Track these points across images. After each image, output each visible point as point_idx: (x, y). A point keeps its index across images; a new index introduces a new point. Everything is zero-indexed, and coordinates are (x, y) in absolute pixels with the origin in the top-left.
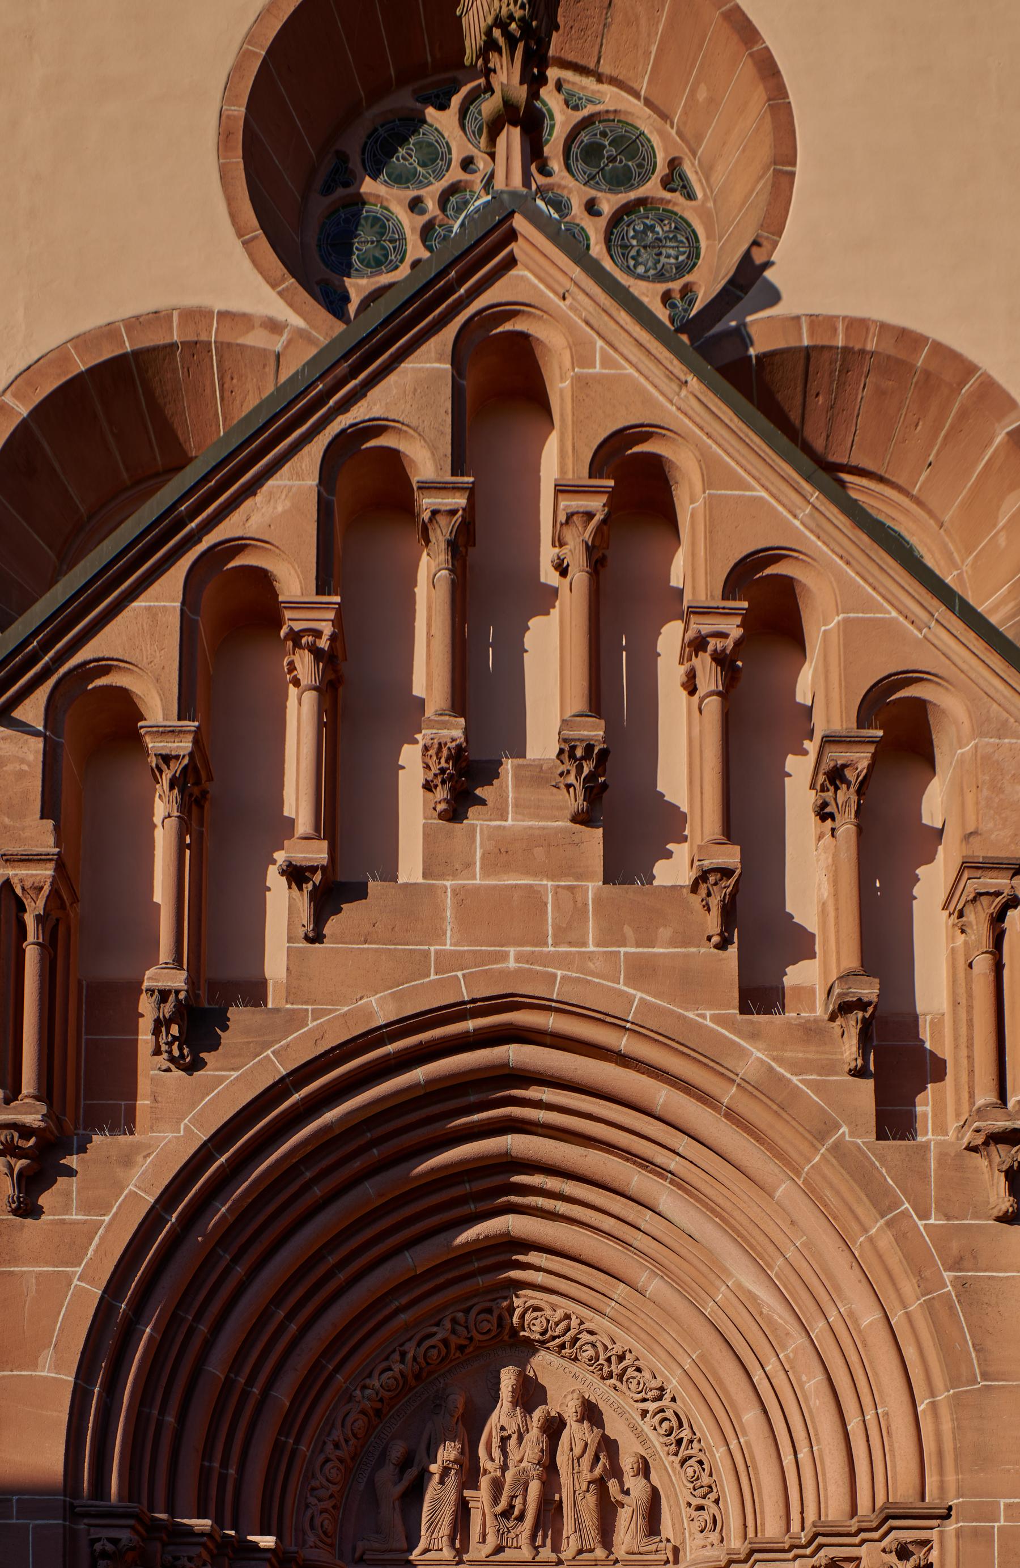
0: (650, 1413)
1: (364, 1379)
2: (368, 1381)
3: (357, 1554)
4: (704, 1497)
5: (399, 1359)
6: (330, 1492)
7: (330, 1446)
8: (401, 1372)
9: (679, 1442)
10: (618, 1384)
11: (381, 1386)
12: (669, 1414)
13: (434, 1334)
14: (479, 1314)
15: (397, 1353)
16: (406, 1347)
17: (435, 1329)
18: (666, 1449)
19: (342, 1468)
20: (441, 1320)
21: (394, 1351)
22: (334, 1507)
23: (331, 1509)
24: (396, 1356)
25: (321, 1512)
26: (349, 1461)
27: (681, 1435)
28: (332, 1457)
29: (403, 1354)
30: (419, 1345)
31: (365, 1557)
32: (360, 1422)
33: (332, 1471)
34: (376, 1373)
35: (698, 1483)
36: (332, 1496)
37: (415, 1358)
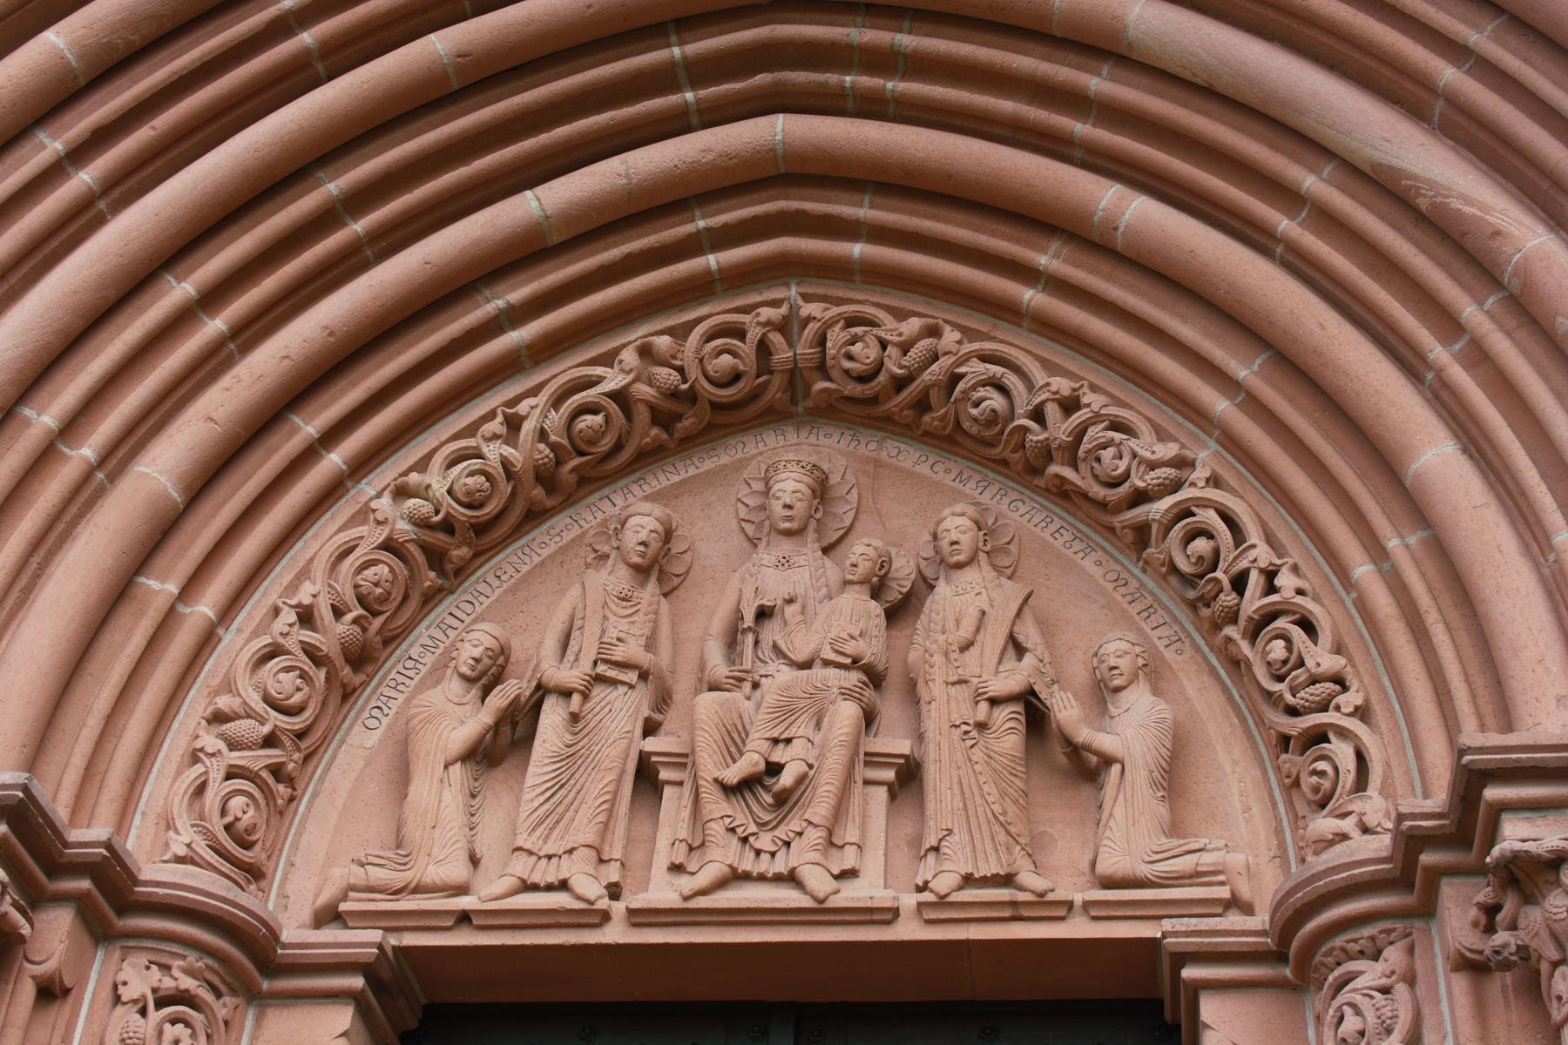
0: (1155, 527)
1: (406, 473)
2: (414, 478)
3: (323, 899)
4: (1325, 709)
5: (503, 430)
6: (266, 729)
8: (506, 464)
9: (1239, 583)
10: (1068, 473)
11: (449, 492)
12: (1211, 518)
13: (596, 381)
14: (710, 338)
15: (500, 418)
16: (523, 407)
17: (599, 370)
18: (1205, 612)
20: (616, 352)
21: (491, 416)
22: (277, 771)
23: (265, 774)
24: (496, 426)
25: (229, 777)
26: (339, 661)
27: (1243, 564)
28: (290, 644)
29: (514, 424)
30: (557, 402)
31: (343, 907)
32: (383, 570)
33: (282, 676)
34: (438, 460)
35: (1300, 675)
36: (270, 741)
37: (542, 435)
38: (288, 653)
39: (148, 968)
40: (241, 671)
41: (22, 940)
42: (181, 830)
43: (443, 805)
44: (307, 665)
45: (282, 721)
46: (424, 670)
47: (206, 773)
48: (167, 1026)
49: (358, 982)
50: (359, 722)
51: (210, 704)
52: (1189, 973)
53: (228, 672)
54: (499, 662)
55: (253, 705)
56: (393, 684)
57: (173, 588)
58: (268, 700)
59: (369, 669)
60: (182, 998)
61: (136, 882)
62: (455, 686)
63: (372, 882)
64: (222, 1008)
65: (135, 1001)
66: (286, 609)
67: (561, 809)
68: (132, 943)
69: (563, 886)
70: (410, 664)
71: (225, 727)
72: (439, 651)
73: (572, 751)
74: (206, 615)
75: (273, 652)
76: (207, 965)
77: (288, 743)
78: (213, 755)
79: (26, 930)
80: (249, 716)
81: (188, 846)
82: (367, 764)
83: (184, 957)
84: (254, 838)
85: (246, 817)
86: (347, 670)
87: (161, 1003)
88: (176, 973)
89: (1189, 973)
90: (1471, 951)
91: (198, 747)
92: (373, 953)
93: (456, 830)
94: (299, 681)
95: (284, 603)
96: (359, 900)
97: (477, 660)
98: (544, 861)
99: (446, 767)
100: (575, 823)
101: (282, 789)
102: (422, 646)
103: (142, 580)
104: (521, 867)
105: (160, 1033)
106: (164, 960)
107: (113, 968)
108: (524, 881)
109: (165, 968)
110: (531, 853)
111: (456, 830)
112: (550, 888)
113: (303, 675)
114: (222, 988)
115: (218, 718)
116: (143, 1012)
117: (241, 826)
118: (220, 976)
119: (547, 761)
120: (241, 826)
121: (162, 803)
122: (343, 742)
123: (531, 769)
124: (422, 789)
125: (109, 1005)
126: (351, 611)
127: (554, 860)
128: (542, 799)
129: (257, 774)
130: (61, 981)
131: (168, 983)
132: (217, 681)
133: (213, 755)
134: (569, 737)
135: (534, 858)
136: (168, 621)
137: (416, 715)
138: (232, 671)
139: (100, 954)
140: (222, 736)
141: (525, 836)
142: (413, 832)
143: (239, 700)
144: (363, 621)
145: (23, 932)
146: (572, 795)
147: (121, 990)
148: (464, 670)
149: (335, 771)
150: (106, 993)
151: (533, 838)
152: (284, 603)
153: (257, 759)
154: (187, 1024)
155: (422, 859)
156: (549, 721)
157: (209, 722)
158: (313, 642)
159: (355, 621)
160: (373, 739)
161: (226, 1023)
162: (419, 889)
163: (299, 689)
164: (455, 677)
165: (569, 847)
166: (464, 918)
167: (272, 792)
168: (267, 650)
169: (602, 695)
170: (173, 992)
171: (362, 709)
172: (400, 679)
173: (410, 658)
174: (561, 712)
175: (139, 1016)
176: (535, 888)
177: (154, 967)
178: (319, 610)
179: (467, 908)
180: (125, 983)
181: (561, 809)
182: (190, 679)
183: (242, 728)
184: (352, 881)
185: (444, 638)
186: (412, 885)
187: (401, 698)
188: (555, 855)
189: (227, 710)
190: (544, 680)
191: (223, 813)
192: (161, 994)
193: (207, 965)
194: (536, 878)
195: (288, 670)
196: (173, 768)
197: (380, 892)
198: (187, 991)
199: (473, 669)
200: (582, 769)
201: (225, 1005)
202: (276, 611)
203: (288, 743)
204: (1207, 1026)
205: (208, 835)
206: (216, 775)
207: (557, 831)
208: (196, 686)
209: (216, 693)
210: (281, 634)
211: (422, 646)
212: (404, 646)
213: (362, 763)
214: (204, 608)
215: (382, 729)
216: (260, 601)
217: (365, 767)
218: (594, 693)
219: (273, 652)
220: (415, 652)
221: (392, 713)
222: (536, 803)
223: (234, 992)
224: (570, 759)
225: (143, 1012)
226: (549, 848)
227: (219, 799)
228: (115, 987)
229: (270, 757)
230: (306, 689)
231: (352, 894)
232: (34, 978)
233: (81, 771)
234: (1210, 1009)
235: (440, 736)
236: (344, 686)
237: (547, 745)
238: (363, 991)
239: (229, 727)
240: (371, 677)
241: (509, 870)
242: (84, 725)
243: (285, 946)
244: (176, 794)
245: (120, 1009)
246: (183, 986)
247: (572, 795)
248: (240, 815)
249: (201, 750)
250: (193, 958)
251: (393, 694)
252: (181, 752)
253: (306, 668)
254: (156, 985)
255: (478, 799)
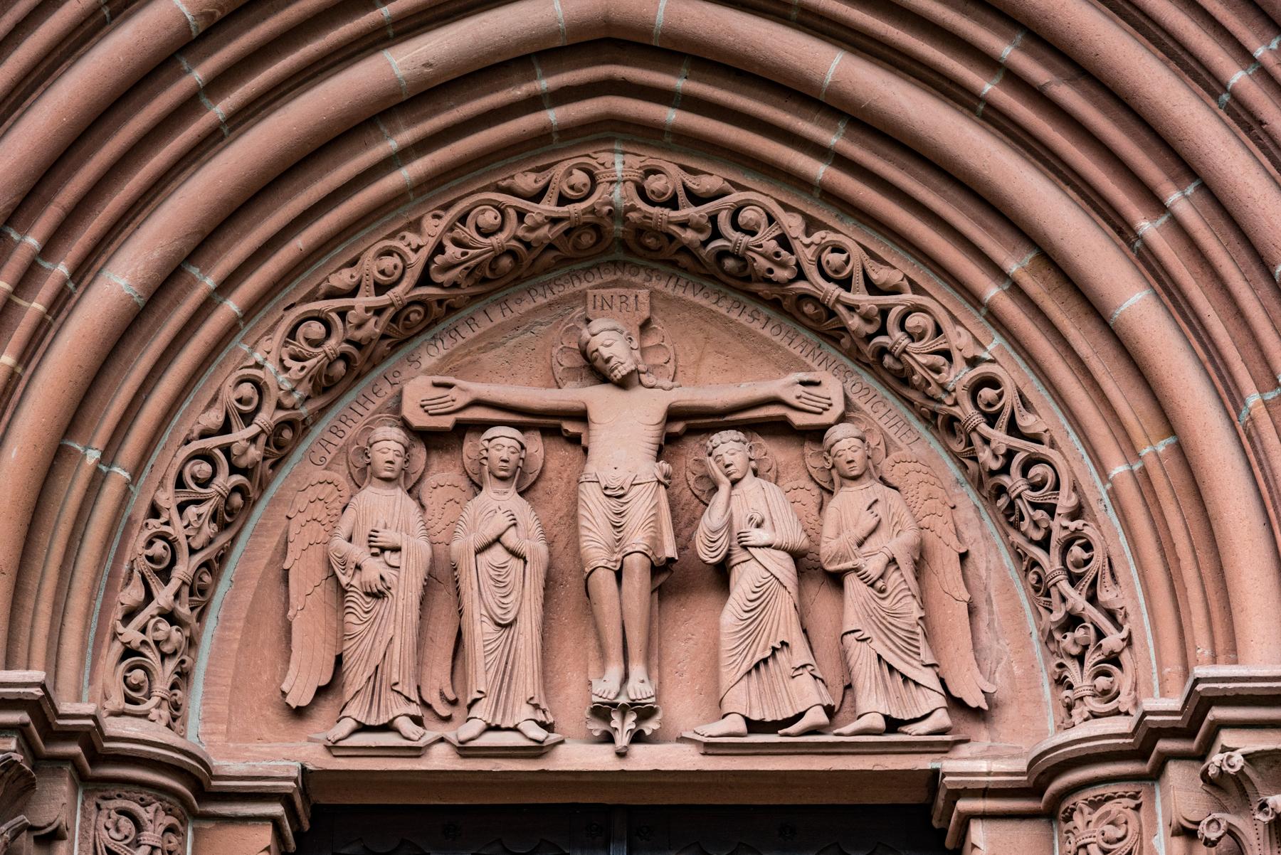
49: (277, 809)
52: (963, 805)
89: (963, 805)
90: (1186, 820)
92: (291, 787)
204: (974, 846)
234: (978, 832)
238: (283, 816)
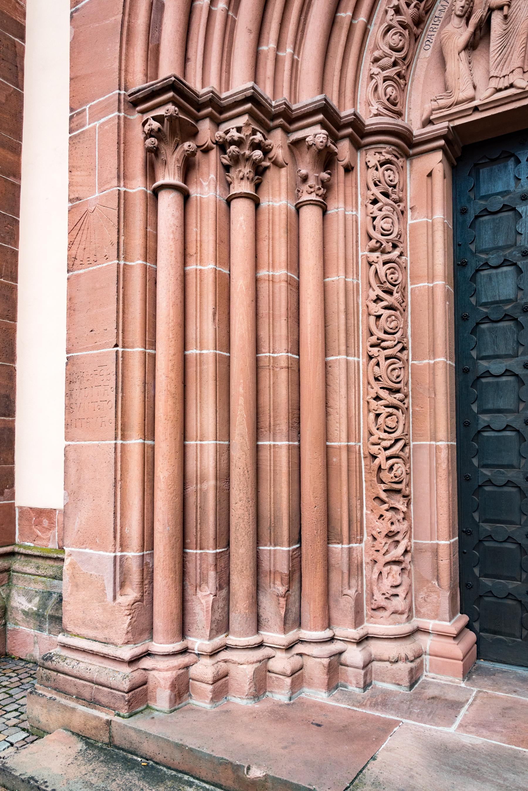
3: (424, 117)
6: (393, 59)
7: (391, 12)
19: (406, 33)
22: (399, 74)
23: (396, 77)
25: (384, 81)
26: (412, 25)
28: (394, 23)
31: (432, 117)
33: (394, 37)
36: (395, 64)
38: (394, 27)
39: (375, 154)
40: (379, 40)
41: (336, 154)
42: (373, 105)
43: (461, 69)
44: (401, 30)
45: (395, 55)
46: (442, 20)
47: (377, 82)
48: (385, 172)
49: (442, 142)
50: (422, 49)
51: (372, 56)
53: (375, 42)
54: (471, 5)
55: (386, 51)
56: (431, 29)
57: (350, 14)
58: (392, 48)
59: (422, 26)
60: (388, 162)
61: (364, 126)
62: (456, 21)
63: (440, 106)
64: (400, 162)
65: (374, 166)
66: (390, 9)
67: (506, 56)
68: (368, 148)
69: (512, 86)
70: (436, 19)
71: (379, 63)
72: (446, 10)
73: (506, 31)
74: (363, 21)
75: (389, 28)
76: (393, 149)
77: (401, 63)
78: (377, 74)
79: (336, 151)
80: (386, 56)
81: (377, 109)
82: (428, 64)
83: (385, 148)
84: (397, 102)
85: (393, 94)
86: (415, 28)
87: (382, 165)
88: (384, 154)
91: (372, 73)
93: (467, 77)
94: (400, 37)
95: (389, 7)
96: (437, 114)
97: (463, 7)
98: (502, 79)
99: (459, 54)
100: (512, 60)
101: (402, 81)
102: (439, 10)
103: (339, 14)
104: (494, 83)
105: (384, 175)
106: (379, 150)
107: (364, 158)
108: (496, 89)
109: (380, 153)
110: (497, 77)
111: (467, 77)
112: (506, 88)
113: (401, 35)
114: (398, 156)
115: (376, 60)
116: (377, 169)
117: (392, 98)
118: (397, 152)
119: (498, 39)
120: (392, 98)
121: (365, 97)
122: (418, 58)
123: (492, 44)
124: (451, 65)
125: (366, 170)
126: (413, 2)
127: (506, 77)
128: (498, 55)
129: (393, 78)
130: (351, 165)
131: (382, 158)
132: (372, 46)
133: (377, 74)
134: (504, 26)
135: (498, 79)
136: (351, 26)
137: (443, 38)
138: (376, 41)
139: (359, 154)
140: (378, 67)
141: (494, 71)
142: (451, 82)
143: (381, 51)
144: (417, 6)
145: (336, 151)
146: (509, 49)
147: (368, 164)
148: (459, 13)
149: (417, 70)
150: (364, 166)
151: (497, 71)
152: (389, 7)
153: (392, 72)
154: (391, 170)
155: (457, 91)
156: (495, 22)
157: (373, 63)
158: (402, 20)
159: (415, 6)
160: (428, 53)
161: (402, 167)
162: (457, 103)
163: (401, 40)
164: (455, 17)
165: (511, 70)
166: (476, 109)
167: (399, 83)
168: (386, 28)
169: (516, 4)
170: (384, 161)
171: (422, 43)
172: (434, 26)
173: (436, 17)
174: (500, 17)
175: (376, 171)
176: (500, 90)
177: (377, 154)
178: (402, 6)
179: (477, 105)
180: (369, 161)
181: (506, 56)
182: (363, 49)
183: (385, 61)
184: (433, 107)
185: (447, 4)
186: (455, 103)
187: (436, 34)
188: (506, 75)
189: (378, 56)
190: (491, 5)
191: (386, 95)
192: (381, 162)
193: (393, 149)
194: (501, 86)
195: (395, 34)
196: (365, 83)
197: (444, 108)
198: (389, 159)
199: (462, 11)
200: (512, 37)
201: (400, 161)
202: (386, 12)
203: (401, 63)
205: (382, 104)
206: (380, 81)
207: (505, 65)
208: (366, 51)
209: (373, 51)
210: (390, 20)
211: (439, 10)
212: (433, 13)
213: (426, 64)
214: (362, 18)
215: (431, 48)
216: (379, 10)
217: (428, 65)
218: (512, 4)
219: (389, 28)
220: (437, 14)
221: (433, 41)
222: (496, 57)
223: (402, 156)
224: (506, 35)
225: (377, 169)
226: (504, 73)
227: (383, 90)
228: (366, 163)
229: (396, 70)
230: (403, 40)
231: (434, 112)
232: (342, 166)
233: (338, 93)
235: (454, 44)
236: (415, 35)
237: (497, 32)
238: (444, 145)
239: (381, 63)
240: (423, 29)
241: (490, 86)
242: (334, 75)
243: (415, 137)
244: (369, 93)
245: (369, 170)
246: (387, 158)
247: (509, 49)
248: (391, 94)
249: (373, 74)
250: (389, 148)
251: (432, 33)
252: (366, 77)
253: (401, 31)
254: (379, 159)
255: (471, 64)
